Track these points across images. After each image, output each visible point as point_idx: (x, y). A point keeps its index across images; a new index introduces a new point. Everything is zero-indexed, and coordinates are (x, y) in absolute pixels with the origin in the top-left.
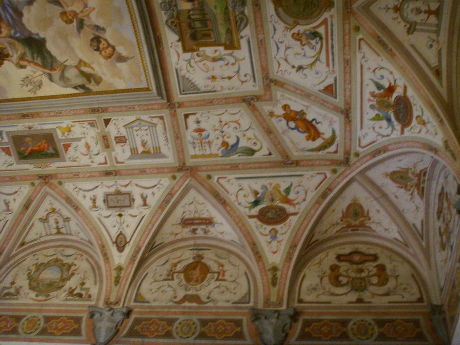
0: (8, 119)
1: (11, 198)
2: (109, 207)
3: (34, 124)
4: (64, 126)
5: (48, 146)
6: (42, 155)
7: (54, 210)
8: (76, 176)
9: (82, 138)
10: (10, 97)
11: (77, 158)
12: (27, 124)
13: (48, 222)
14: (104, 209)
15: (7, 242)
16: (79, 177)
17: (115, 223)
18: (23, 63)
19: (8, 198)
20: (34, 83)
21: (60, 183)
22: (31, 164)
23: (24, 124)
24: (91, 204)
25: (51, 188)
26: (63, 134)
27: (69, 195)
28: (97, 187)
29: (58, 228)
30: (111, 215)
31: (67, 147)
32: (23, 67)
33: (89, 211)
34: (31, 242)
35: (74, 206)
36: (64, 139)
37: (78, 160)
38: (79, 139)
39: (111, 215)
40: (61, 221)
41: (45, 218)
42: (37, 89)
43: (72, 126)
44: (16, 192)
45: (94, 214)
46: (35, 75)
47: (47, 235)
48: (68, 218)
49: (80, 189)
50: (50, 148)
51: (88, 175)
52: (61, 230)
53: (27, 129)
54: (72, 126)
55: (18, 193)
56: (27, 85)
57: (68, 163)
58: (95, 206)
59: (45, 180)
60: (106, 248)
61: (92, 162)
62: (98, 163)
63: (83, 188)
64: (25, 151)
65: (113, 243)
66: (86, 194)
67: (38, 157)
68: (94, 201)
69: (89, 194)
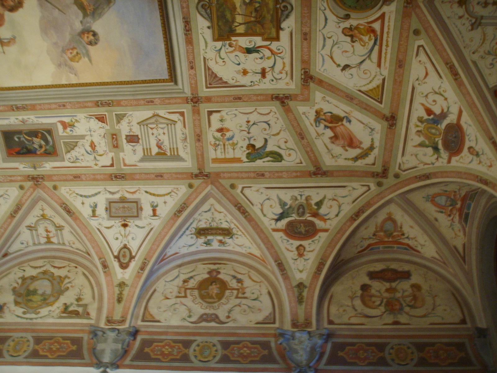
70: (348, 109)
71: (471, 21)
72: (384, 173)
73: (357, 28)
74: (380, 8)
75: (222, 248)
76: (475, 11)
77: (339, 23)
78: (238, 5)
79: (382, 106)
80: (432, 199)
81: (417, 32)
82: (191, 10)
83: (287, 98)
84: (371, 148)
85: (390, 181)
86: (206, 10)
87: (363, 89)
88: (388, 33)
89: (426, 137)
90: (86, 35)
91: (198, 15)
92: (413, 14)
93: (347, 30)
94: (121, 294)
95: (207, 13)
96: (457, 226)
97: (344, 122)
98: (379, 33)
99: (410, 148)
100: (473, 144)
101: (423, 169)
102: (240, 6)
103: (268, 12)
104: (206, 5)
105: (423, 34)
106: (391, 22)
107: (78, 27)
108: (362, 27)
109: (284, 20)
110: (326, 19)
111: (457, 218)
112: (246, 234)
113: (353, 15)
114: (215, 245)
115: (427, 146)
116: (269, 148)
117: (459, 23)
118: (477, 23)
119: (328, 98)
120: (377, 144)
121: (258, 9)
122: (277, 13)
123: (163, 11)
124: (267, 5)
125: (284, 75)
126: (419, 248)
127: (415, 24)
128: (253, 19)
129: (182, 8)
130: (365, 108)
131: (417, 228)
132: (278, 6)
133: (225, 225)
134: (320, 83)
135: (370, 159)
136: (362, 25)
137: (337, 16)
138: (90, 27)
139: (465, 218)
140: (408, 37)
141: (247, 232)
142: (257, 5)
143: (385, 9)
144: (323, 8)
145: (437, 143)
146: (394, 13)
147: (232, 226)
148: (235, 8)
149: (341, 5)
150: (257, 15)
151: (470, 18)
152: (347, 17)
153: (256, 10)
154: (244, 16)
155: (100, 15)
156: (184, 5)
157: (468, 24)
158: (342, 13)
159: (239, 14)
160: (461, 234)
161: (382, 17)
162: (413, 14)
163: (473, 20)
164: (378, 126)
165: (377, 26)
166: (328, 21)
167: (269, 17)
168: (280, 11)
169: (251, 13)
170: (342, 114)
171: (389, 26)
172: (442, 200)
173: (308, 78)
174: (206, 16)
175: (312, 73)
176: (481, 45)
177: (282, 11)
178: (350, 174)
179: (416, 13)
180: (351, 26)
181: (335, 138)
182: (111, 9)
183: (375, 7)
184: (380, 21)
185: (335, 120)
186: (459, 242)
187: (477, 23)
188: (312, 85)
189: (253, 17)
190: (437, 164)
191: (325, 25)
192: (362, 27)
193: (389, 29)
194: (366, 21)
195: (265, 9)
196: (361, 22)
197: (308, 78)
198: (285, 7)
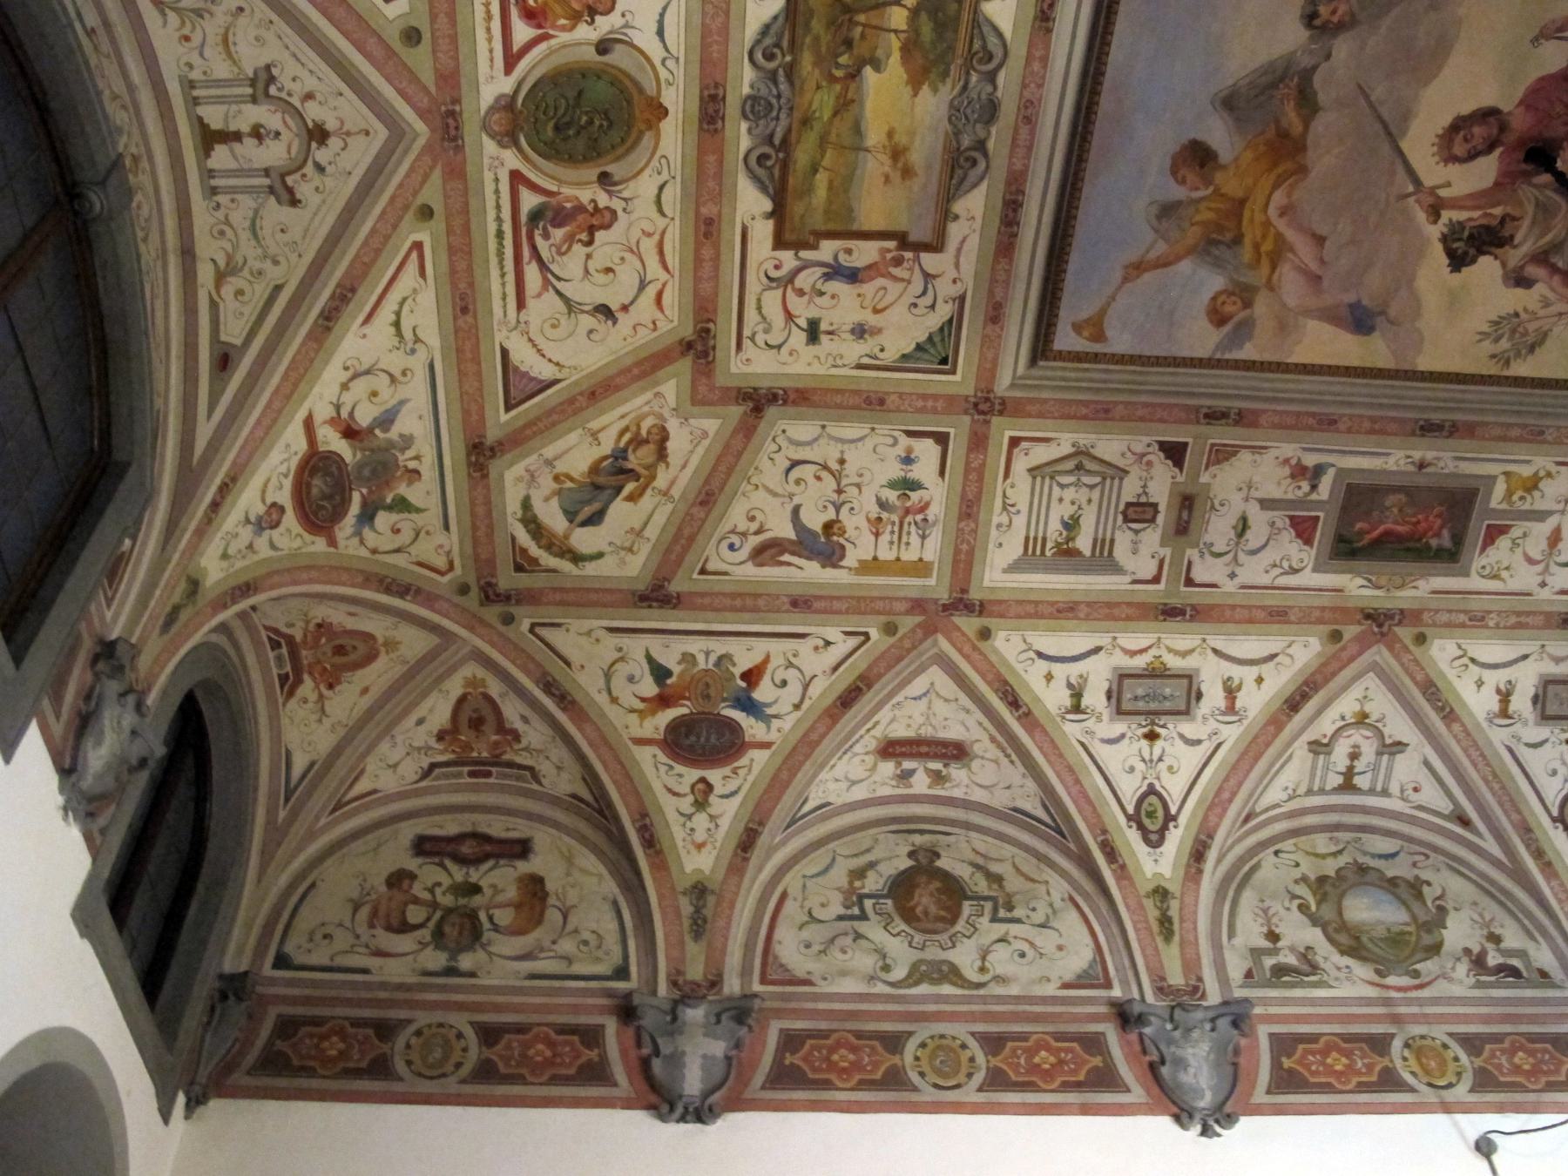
0: (1371, 432)
1: (1249, 673)
2: (1545, 718)
3: (1441, 454)
4: (1526, 471)
5: (1442, 527)
6: (1408, 550)
7: (1362, 719)
8: (1477, 621)
9: (1550, 513)
10: (1421, 368)
11: (1507, 568)
12: (1417, 455)
13: (1329, 754)
14: (1531, 723)
15: (1218, 810)
16: (1486, 627)
17: (1557, 765)
18: (1532, 270)
19: (1236, 672)
20: (1526, 334)
21: (1421, 639)
22: (1359, 574)
23: (1409, 453)
24: (1495, 706)
25: (1391, 649)
26: (1509, 494)
27: (1433, 675)
28: (1525, 657)
29: (1349, 774)
30: (1546, 741)
31: (1494, 534)
32: (1520, 280)
33: (1485, 725)
34: (1267, 810)
35: (1442, 709)
36: (1504, 511)
37: (1504, 574)
38: (1541, 516)
39: (1546, 741)
40: (1369, 750)
41: (1325, 741)
42: (1518, 355)
43: (1549, 475)
44: (1273, 657)
45: (1498, 736)
46: (1541, 313)
47: (1310, 792)
48: (1399, 743)
49: (1473, 660)
50: (1445, 533)
51: (1513, 620)
52: (1357, 780)
53: (1411, 468)
54: (1549, 475)
55: (1277, 660)
56: (1497, 340)
57: (1475, 582)
58: (1504, 713)
59: (1380, 626)
60: (1538, 833)
61: (1543, 584)
62: (1557, 588)
63: (1483, 659)
64: (1361, 533)
65: (1554, 820)
66: (1488, 675)
67: (1392, 557)
68: (1505, 696)
69: (1494, 678)
71: (280, 90)
73: (576, 18)
74: (520, 85)
76: (279, 115)
77: (626, 26)
78: (896, 57)
81: (412, 36)
82: (1023, 52)
86: (984, 47)
88: (489, 17)
90: (1335, 19)
91: (1008, 35)
92: (433, 89)
93: (601, 8)
95: (983, 39)
98: (514, 13)
102: (888, 57)
103: (817, 39)
104: (980, 61)
105: (393, 37)
106: (485, 50)
107: (1342, 47)
108: (562, 22)
109: (775, 18)
110: (660, 33)
113: (590, 54)
117: (310, 83)
118: (260, 85)
121: (843, 48)
122: (792, 42)
123: (1099, 59)
124: (817, 63)
127: (421, 60)
128: (862, 18)
129: (1045, 60)
132: (788, 58)
136: (563, 29)
137: (632, 45)
138: (1311, 38)
140: (433, 18)
142: (843, 60)
143: (506, 85)
144: (670, 63)
146: (481, 79)
148: (905, 50)
149: (622, 77)
150: (849, 30)
151: (284, 95)
152: (603, 47)
153: (848, 43)
154: (886, 26)
155: (1269, 68)
156: (1036, 66)
157: (284, 79)
158: (617, 57)
159: (896, 31)
161: (509, 68)
162: (433, 89)
163: (273, 90)
165: (522, 32)
166: (654, 27)
167: (817, 26)
168: (785, 44)
169: (863, 36)
171: (490, 40)
174: (986, 29)
176: (227, 30)
177: (777, 45)
179: (425, 89)
180: (593, 21)
182: (1230, 82)
183: (535, 86)
184: (515, 49)
187: (260, 85)
189: (858, 23)
191: (662, 15)
192: (562, 22)
193: (488, 30)
194: (553, 42)
195: (824, 49)
196: (564, 37)
198: (769, 57)
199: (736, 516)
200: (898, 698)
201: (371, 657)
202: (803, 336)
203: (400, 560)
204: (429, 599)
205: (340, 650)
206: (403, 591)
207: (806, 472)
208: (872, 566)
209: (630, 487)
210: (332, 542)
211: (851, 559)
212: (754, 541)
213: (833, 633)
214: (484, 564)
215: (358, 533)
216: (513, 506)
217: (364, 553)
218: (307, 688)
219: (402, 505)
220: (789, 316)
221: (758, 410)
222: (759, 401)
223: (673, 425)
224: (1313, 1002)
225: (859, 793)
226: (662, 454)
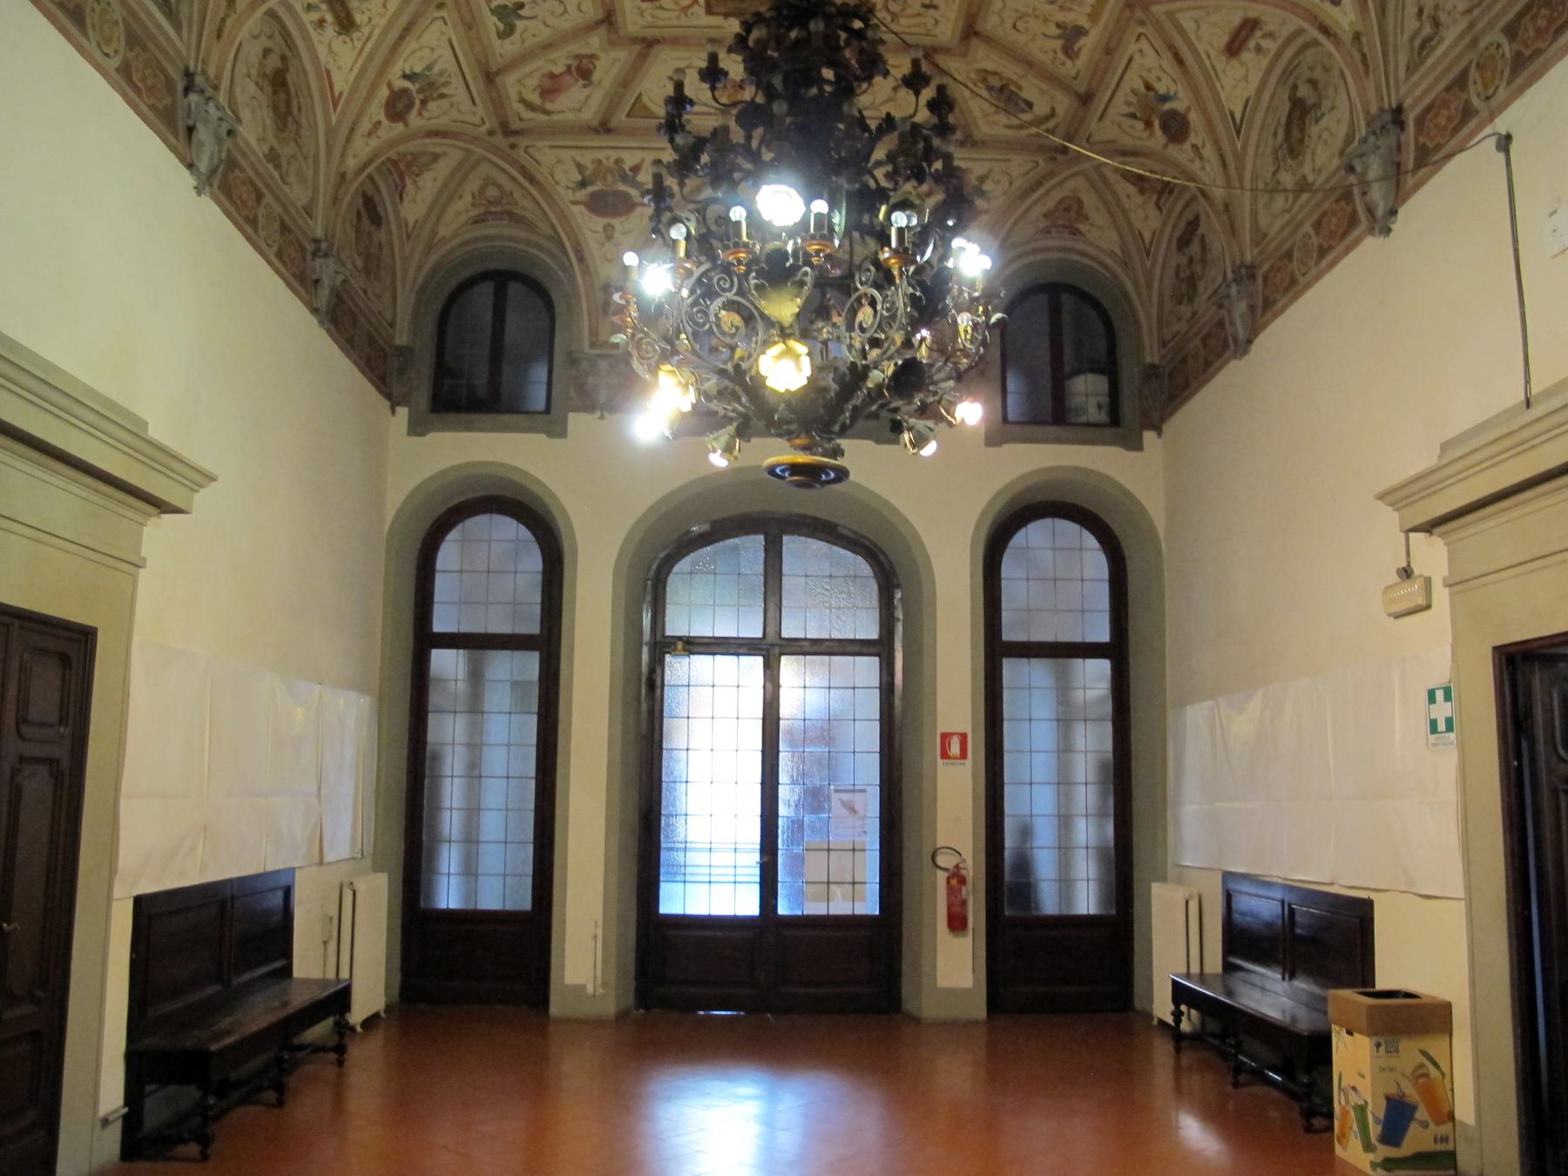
70: (606, 84)
72: (507, 131)
75: (310, 28)
79: (623, 117)
80: (488, 182)
83: (611, 24)
84: (547, 112)
85: (500, 141)
87: (645, 99)
89: (596, 173)
94: (223, 20)
96: (463, 218)
97: (582, 82)
99: (566, 155)
100: (618, 228)
101: (542, 174)
111: (471, 214)
112: (364, 55)
114: (309, 18)
115: (581, 172)
116: (520, 24)
119: (618, 65)
120: (556, 117)
125: (649, 18)
126: (406, 199)
130: (613, 102)
131: (439, 184)
133: (358, 18)
134: (643, 57)
135: (526, 114)
139: (479, 220)
141: (370, 58)
145: (592, 184)
147: (366, 30)
160: (454, 226)
164: (590, 115)
170: (596, 77)
172: (492, 192)
173: (649, 44)
175: (657, 48)
178: (497, 102)
181: (552, 76)
185: (583, 71)
186: (443, 231)
188: (637, 48)
190: (560, 190)
197: (649, 44)
199: (1046, 58)
200: (1193, 38)
201: (1080, 202)
202: (932, 12)
203: (1017, 184)
204: (1051, 174)
205: (1067, 210)
206: (1039, 184)
207: (1020, 25)
208: (1094, 17)
209: (1012, 88)
210: (986, 212)
211: (1086, 25)
212: (1060, 55)
213: (1133, 47)
214: (1041, 149)
215: (989, 199)
216: (1010, 133)
217: (1002, 199)
218: (1083, 227)
219: (982, 179)
220: (919, 15)
221: (976, 34)
222: (970, 31)
223: (977, 66)
224: (1439, 61)
225: (1255, 79)
226: (994, 73)
